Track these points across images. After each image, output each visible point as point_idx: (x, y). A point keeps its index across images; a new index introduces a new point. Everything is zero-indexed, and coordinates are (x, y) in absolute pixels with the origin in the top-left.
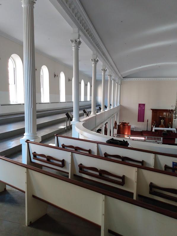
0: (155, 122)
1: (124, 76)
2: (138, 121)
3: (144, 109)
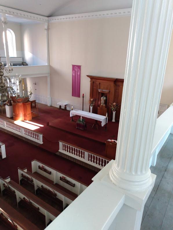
1: (47, 14)
3: (80, 75)
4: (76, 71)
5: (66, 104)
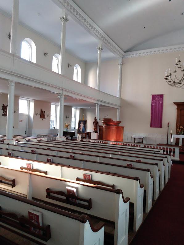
0: (181, 127)
1: (125, 50)
2: (151, 126)
3: (162, 104)
4: (157, 100)
5: (142, 135)
